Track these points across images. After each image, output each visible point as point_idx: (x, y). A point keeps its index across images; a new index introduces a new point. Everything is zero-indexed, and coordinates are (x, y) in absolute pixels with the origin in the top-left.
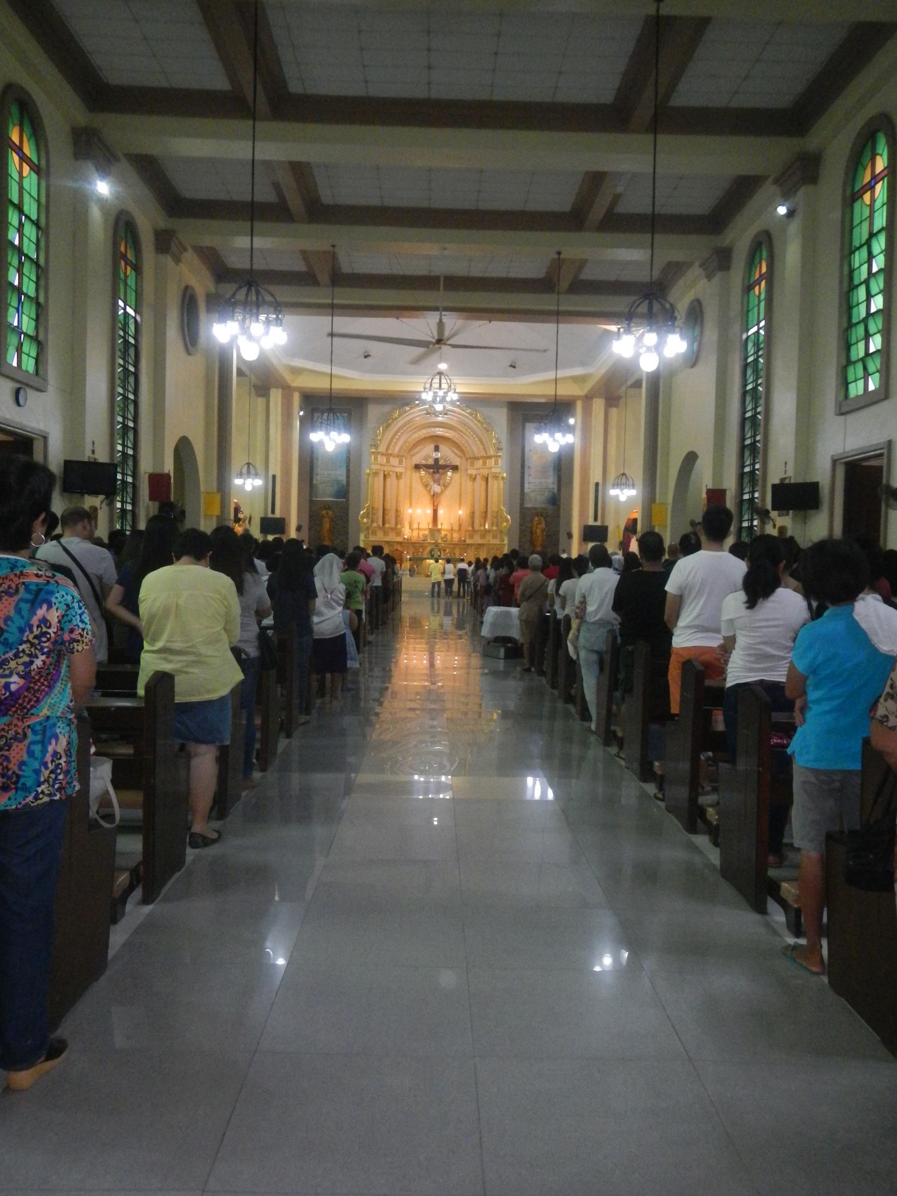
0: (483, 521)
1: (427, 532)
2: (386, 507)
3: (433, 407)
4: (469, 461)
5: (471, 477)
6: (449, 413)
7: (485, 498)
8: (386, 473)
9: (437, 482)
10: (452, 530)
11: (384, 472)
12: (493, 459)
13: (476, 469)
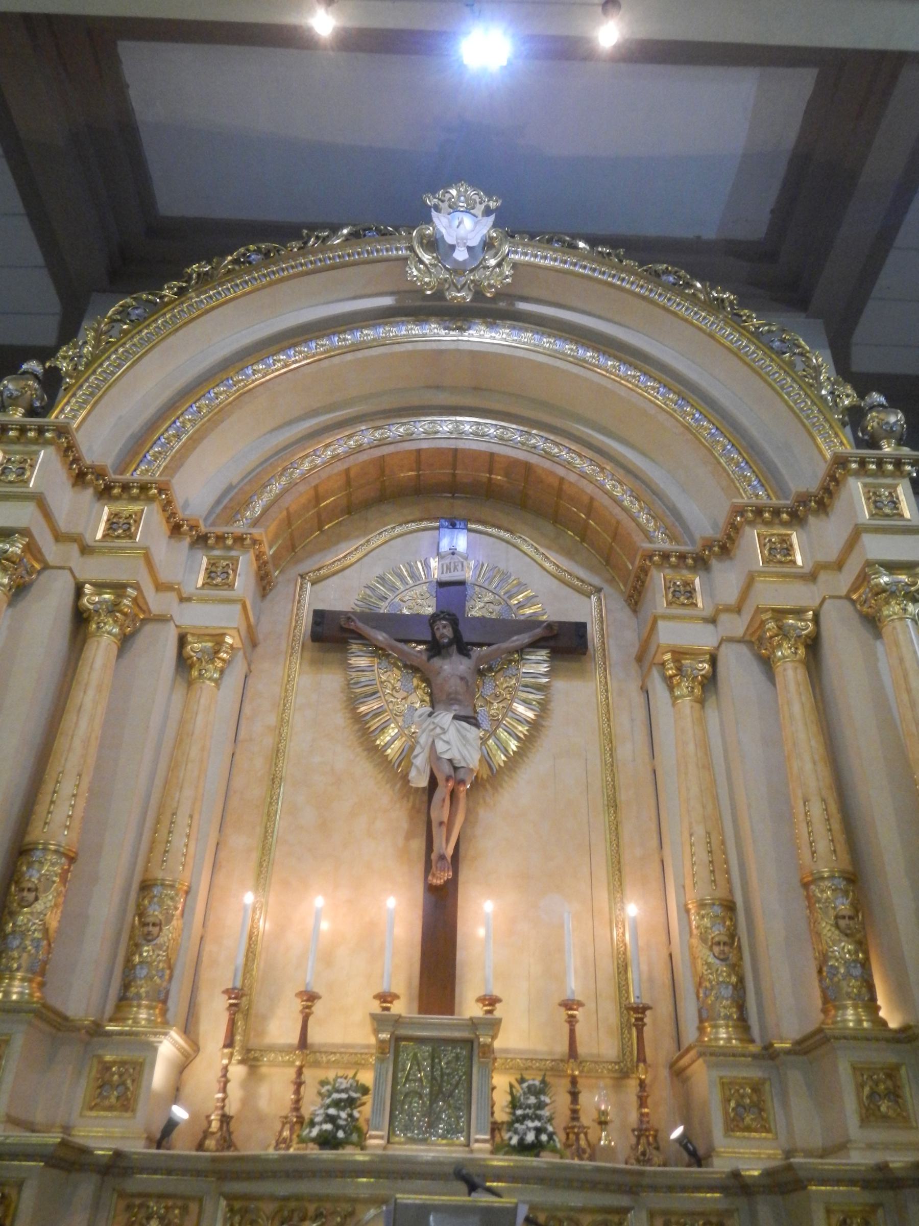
0: (843, 949)
1: (367, 1077)
2: (36, 833)
3: (434, 244)
4: (659, 579)
5: (679, 669)
6: (522, 306)
7: (824, 771)
8: (90, 598)
9: (451, 700)
10: (573, 1052)
11: (79, 592)
12: (856, 487)
13: (713, 621)
